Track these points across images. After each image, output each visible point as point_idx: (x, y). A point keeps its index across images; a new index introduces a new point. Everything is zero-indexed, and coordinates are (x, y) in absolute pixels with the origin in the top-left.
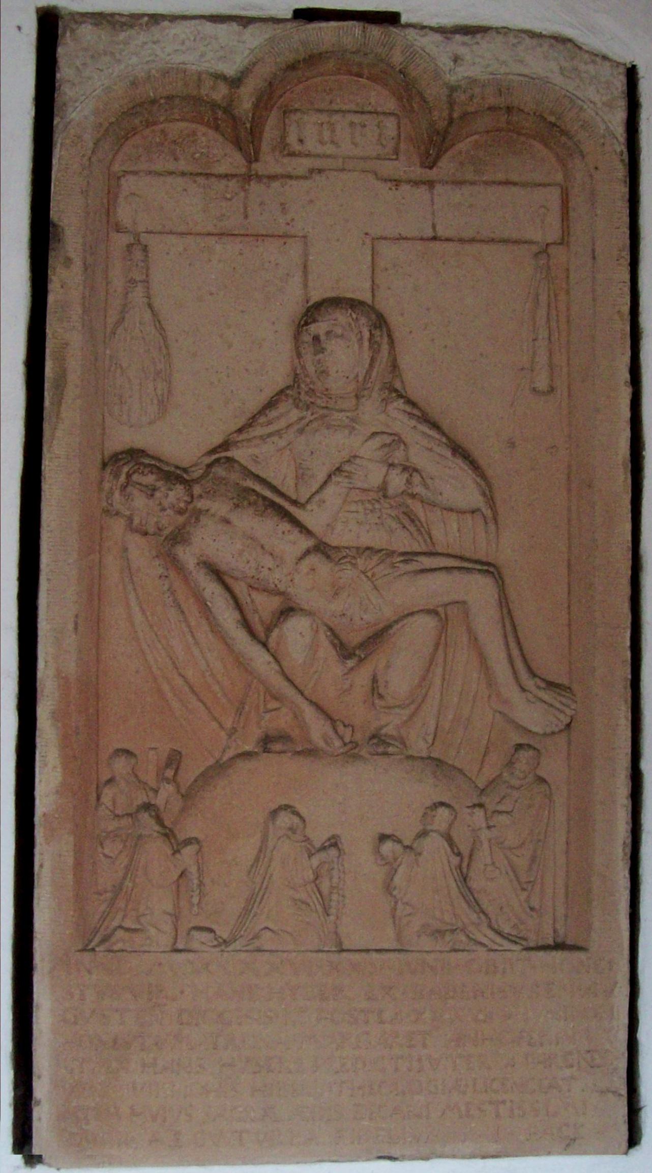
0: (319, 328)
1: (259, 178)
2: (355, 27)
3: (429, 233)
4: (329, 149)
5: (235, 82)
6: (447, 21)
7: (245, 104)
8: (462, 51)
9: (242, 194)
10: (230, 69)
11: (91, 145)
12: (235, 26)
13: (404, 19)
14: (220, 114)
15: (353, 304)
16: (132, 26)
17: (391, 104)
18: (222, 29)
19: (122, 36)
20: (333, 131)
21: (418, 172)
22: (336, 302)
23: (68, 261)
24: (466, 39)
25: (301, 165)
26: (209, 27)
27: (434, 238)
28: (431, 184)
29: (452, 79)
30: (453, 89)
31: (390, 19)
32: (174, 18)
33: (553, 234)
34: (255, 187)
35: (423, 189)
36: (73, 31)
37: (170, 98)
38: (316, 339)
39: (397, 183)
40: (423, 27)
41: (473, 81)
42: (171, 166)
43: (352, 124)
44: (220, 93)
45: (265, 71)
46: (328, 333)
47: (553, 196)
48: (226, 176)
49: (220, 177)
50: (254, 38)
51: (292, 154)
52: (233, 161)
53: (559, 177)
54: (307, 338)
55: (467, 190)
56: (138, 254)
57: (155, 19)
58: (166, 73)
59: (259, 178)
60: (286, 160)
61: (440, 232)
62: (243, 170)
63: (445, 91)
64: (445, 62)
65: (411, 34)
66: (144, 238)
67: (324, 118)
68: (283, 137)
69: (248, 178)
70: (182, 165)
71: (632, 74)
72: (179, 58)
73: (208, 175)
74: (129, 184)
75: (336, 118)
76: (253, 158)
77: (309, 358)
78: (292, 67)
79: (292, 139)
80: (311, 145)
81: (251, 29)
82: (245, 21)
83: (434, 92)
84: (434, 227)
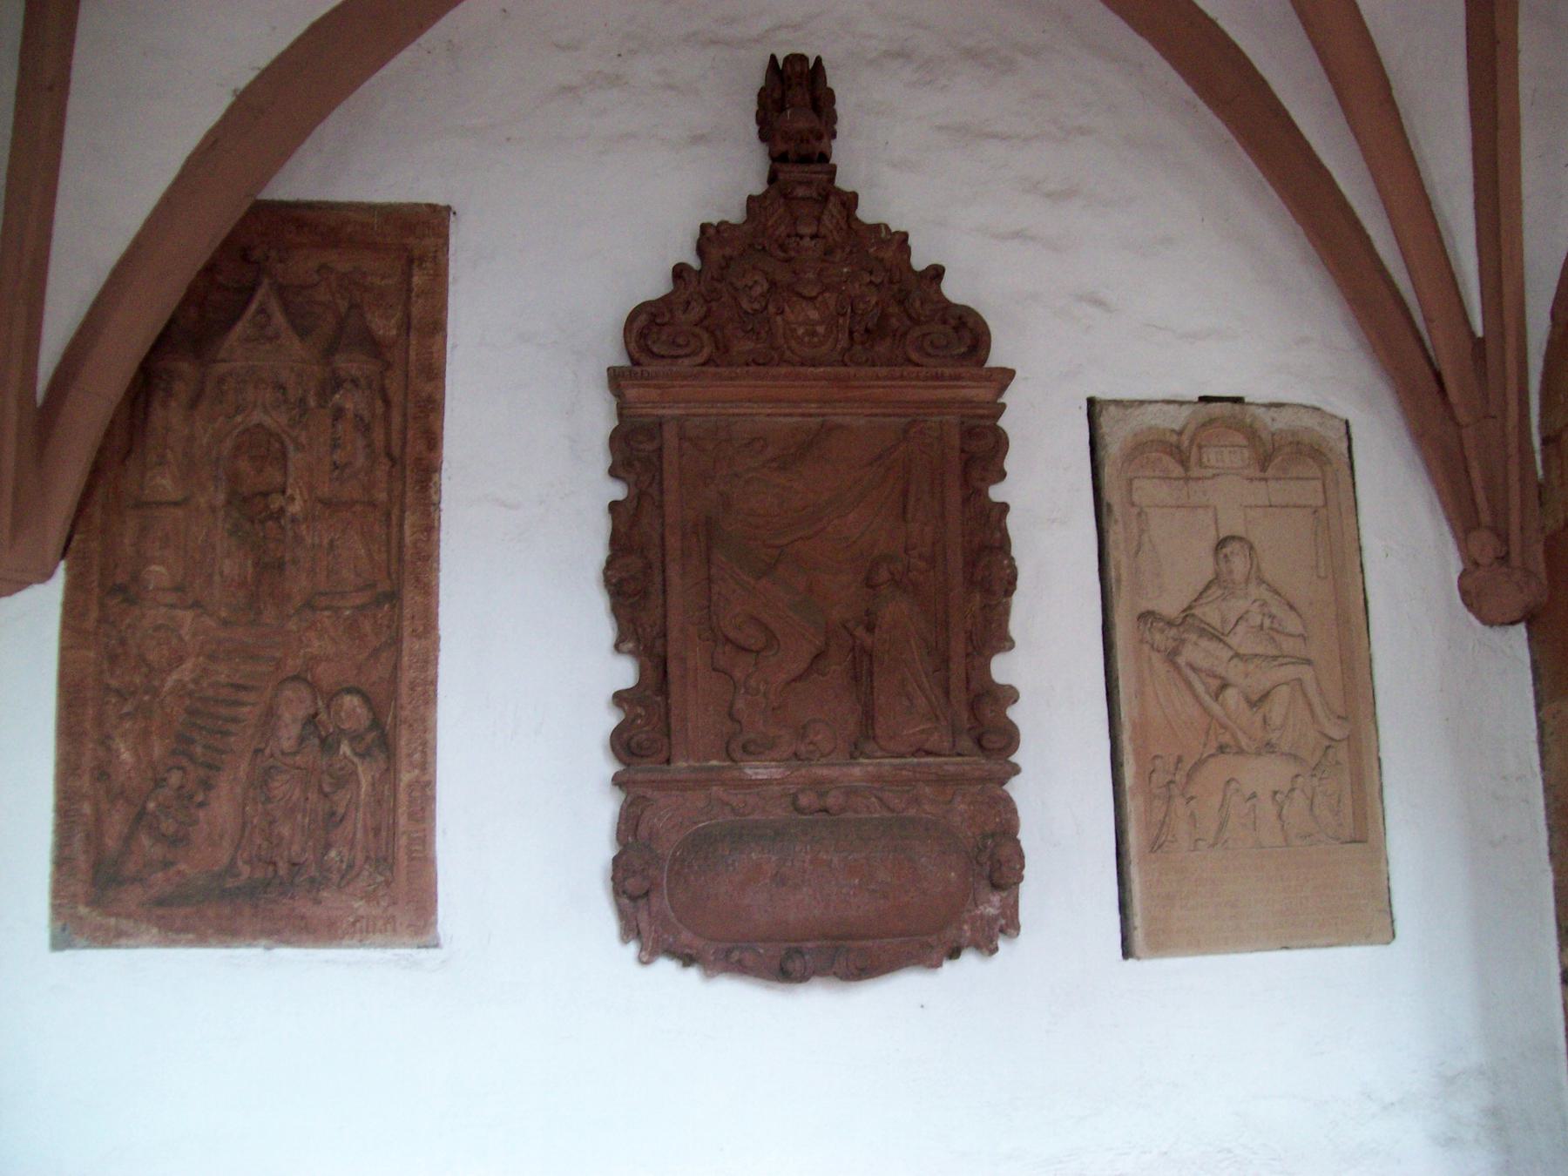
0: (1227, 550)
1: (1192, 479)
2: (1229, 405)
3: (1267, 503)
4: (1221, 464)
5: (1180, 433)
6: (1266, 400)
7: (1186, 443)
8: (1275, 415)
9: (1186, 488)
10: (1177, 427)
11: (1120, 465)
12: (1176, 406)
13: (1247, 400)
14: (1174, 448)
15: (1241, 539)
16: (1131, 407)
17: (1245, 443)
18: (1171, 407)
19: (1130, 410)
20: (1222, 455)
21: (1259, 474)
22: (1232, 538)
23: (1116, 521)
24: (1275, 409)
25: (1209, 472)
26: (1166, 407)
27: (1271, 506)
28: (1266, 480)
29: (1273, 429)
30: (1273, 435)
31: (1237, 400)
32: (1151, 402)
33: (1320, 502)
34: (1192, 483)
35: (1263, 483)
36: (1106, 409)
37: (1152, 441)
38: (1226, 556)
39: (1251, 480)
40: (1257, 405)
41: (1281, 431)
42: (1152, 474)
43: (1230, 452)
44: (1174, 438)
45: (1192, 427)
46: (1232, 553)
47: (1318, 484)
48: (1179, 479)
49: (1175, 479)
50: (1185, 412)
51: (1206, 467)
52: (1178, 471)
53: (1319, 475)
54: (1221, 556)
55: (1282, 482)
56: (1143, 517)
57: (1142, 402)
58: (1150, 428)
59: (1192, 479)
60: (1203, 470)
61: (1272, 504)
62: (1184, 475)
63: (1270, 435)
64: (1268, 420)
65: (1253, 407)
66: (1147, 510)
67: (1217, 449)
68: (1200, 459)
69: (1187, 479)
70: (1157, 473)
71: (1347, 423)
72: (1153, 422)
73: (1170, 478)
74: (1136, 483)
75: (1223, 449)
76: (1187, 469)
77: (1222, 564)
78: (1204, 425)
79: (1205, 460)
80: (1213, 462)
81: (1184, 407)
82: (1181, 403)
83: (1265, 435)
84: (1269, 500)
